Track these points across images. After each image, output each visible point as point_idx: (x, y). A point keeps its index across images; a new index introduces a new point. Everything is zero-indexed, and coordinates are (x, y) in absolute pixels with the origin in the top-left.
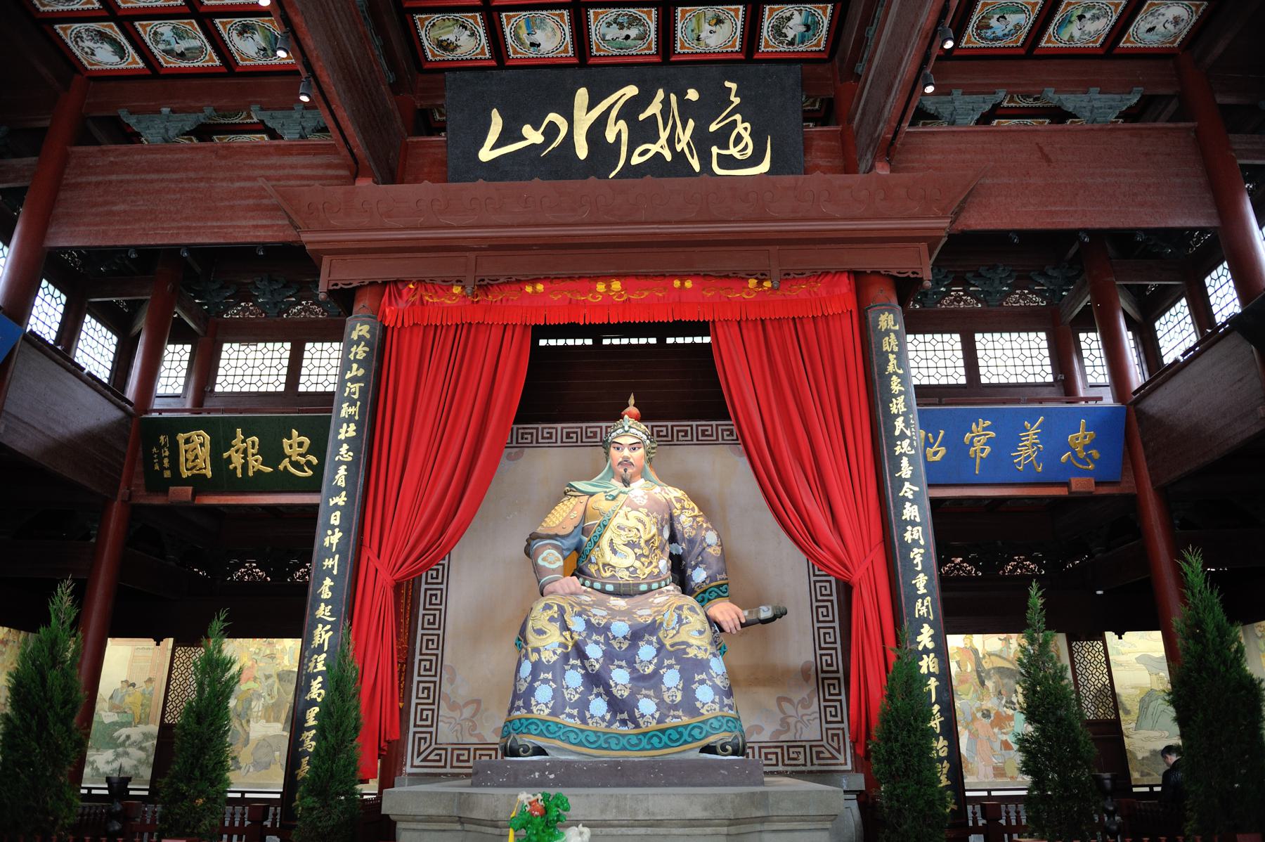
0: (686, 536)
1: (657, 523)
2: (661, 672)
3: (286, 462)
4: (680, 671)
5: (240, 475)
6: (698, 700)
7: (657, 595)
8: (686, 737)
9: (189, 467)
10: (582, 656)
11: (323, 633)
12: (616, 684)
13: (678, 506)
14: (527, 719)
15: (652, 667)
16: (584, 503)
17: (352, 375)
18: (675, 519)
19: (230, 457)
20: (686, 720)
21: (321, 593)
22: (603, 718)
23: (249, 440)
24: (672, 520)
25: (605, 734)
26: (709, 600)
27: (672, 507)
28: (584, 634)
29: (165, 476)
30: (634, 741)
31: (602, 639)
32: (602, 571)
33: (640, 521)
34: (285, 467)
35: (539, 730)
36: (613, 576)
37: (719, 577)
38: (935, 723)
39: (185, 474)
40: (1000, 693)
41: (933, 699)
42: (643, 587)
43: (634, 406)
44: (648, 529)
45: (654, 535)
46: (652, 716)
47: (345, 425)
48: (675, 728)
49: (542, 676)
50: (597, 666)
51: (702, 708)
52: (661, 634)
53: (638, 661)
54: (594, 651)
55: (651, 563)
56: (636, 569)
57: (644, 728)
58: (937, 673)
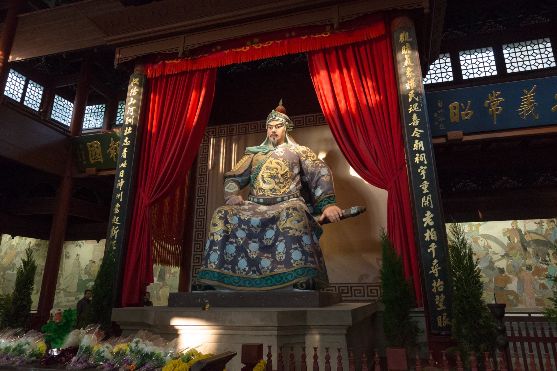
0: (309, 171)
1: (289, 165)
2: (277, 244)
4: (285, 243)
6: (292, 259)
7: (285, 203)
8: (284, 279)
9: (93, 158)
10: (236, 237)
11: (115, 230)
12: (251, 251)
13: (304, 155)
14: (205, 271)
15: (271, 242)
16: (252, 158)
17: (130, 103)
18: (302, 163)
20: (285, 270)
21: (114, 211)
22: (244, 270)
24: (300, 164)
25: (244, 278)
26: (325, 205)
27: (300, 156)
28: (237, 225)
30: (258, 282)
31: (246, 227)
32: (259, 193)
33: (278, 164)
35: (294, 276)
36: (264, 194)
37: (329, 192)
38: (435, 270)
39: (92, 162)
40: (537, 255)
41: (434, 256)
42: (279, 200)
43: (282, 105)
44: (283, 167)
45: (287, 172)
46: (268, 268)
47: (127, 128)
48: (279, 274)
49: (214, 248)
50: (242, 242)
51: (294, 263)
52: (278, 223)
53: (265, 238)
54: (241, 234)
55: (285, 186)
56: (276, 190)
57: (264, 275)
58: (436, 240)
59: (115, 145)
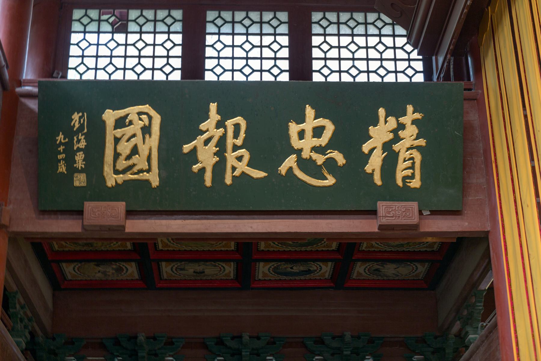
3: (291, 161)
5: (208, 182)
19: (195, 150)
23: (230, 123)
29: (77, 183)
34: (291, 169)
39: (111, 179)
59: (225, 127)
